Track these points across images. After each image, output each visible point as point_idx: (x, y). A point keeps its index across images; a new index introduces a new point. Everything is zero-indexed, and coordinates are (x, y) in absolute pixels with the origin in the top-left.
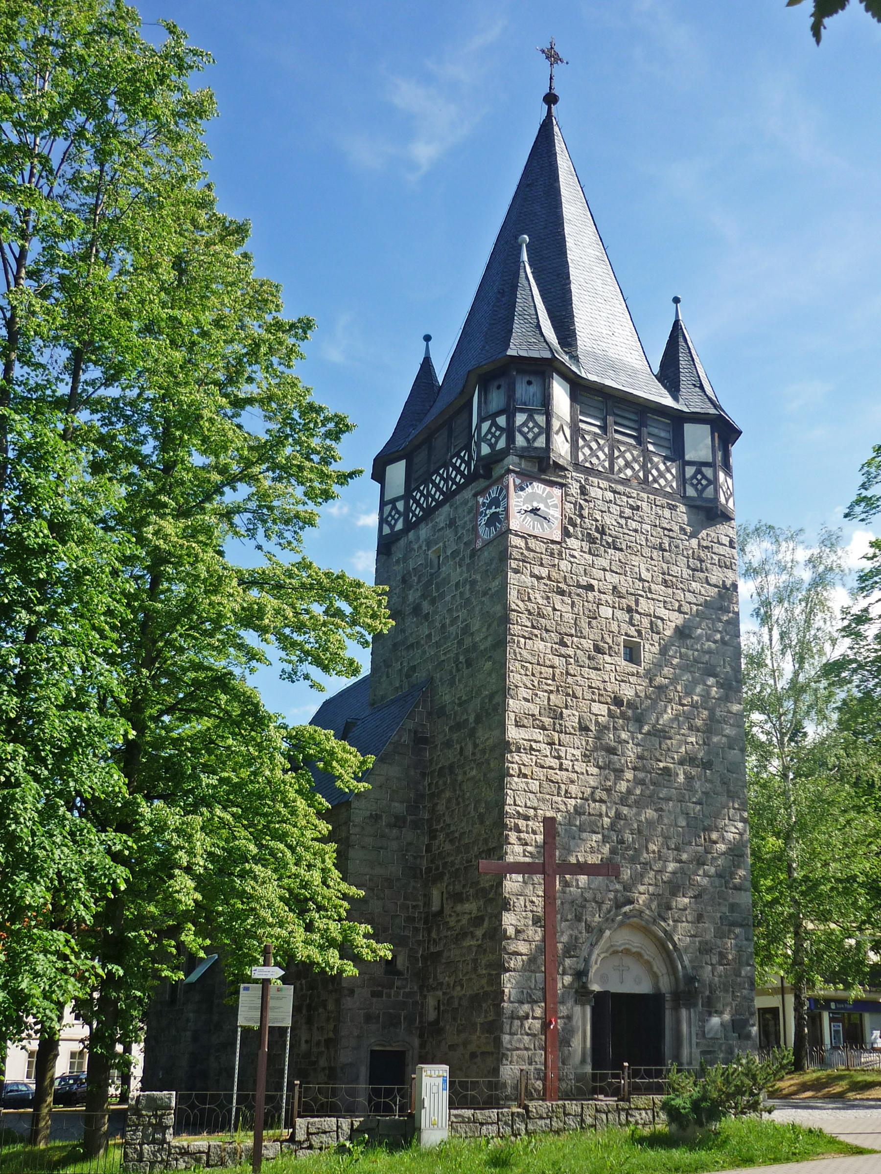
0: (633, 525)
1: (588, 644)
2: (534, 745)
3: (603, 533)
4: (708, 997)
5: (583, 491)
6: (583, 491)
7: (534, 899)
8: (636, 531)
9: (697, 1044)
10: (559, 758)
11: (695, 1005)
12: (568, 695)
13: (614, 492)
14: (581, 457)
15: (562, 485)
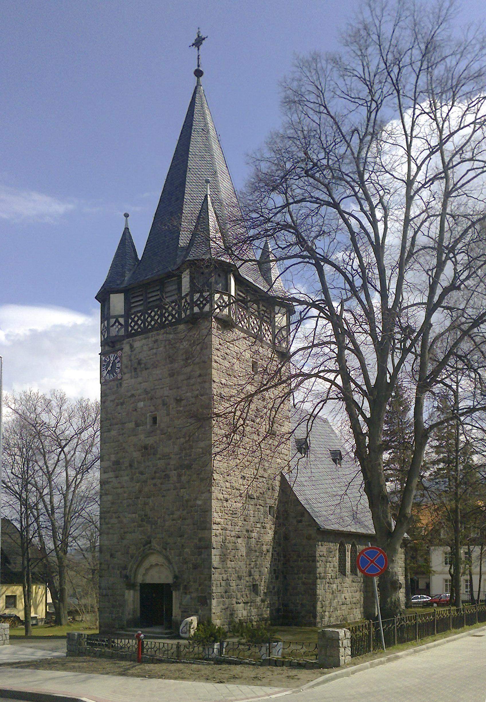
0: (154, 351)
1: (132, 425)
2: (110, 480)
3: (139, 363)
4: (186, 586)
5: (131, 347)
6: (131, 347)
7: (110, 547)
8: (156, 354)
9: (180, 607)
10: (119, 483)
11: (179, 590)
12: (123, 452)
13: (145, 338)
14: (130, 329)
15: (122, 349)
